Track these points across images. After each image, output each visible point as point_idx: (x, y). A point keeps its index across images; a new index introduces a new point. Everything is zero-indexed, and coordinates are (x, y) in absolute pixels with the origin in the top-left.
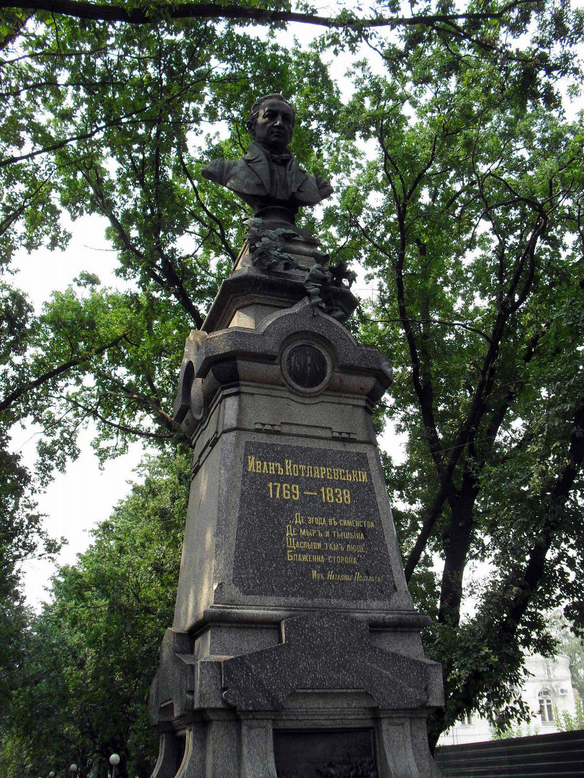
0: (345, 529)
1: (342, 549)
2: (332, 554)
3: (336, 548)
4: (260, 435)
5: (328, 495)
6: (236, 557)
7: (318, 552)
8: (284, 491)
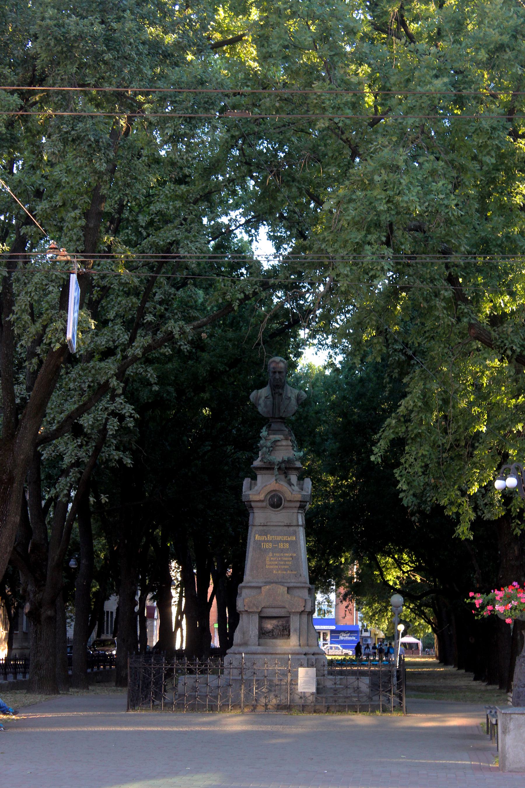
0: (286, 557)
5: (281, 546)
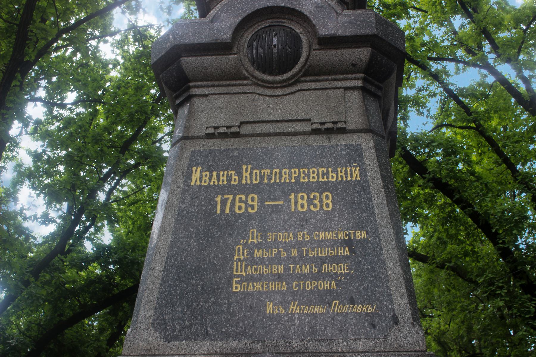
0: (321, 244)
1: (315, 270)
2: (299, 279)
3: (306, 270)
4: (211, 141)
5: (300, 202)
6: (160, 293)
7: (280, 277)
8: (237, 204)
